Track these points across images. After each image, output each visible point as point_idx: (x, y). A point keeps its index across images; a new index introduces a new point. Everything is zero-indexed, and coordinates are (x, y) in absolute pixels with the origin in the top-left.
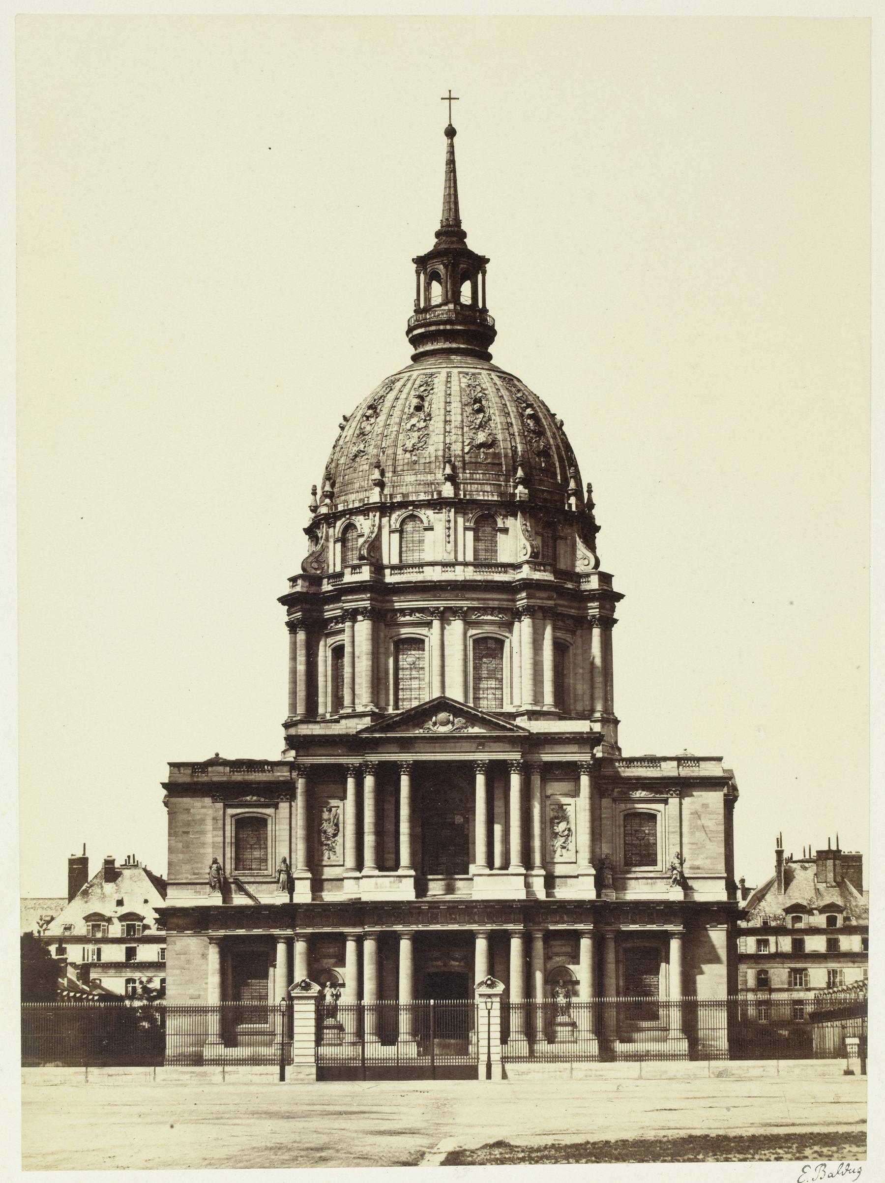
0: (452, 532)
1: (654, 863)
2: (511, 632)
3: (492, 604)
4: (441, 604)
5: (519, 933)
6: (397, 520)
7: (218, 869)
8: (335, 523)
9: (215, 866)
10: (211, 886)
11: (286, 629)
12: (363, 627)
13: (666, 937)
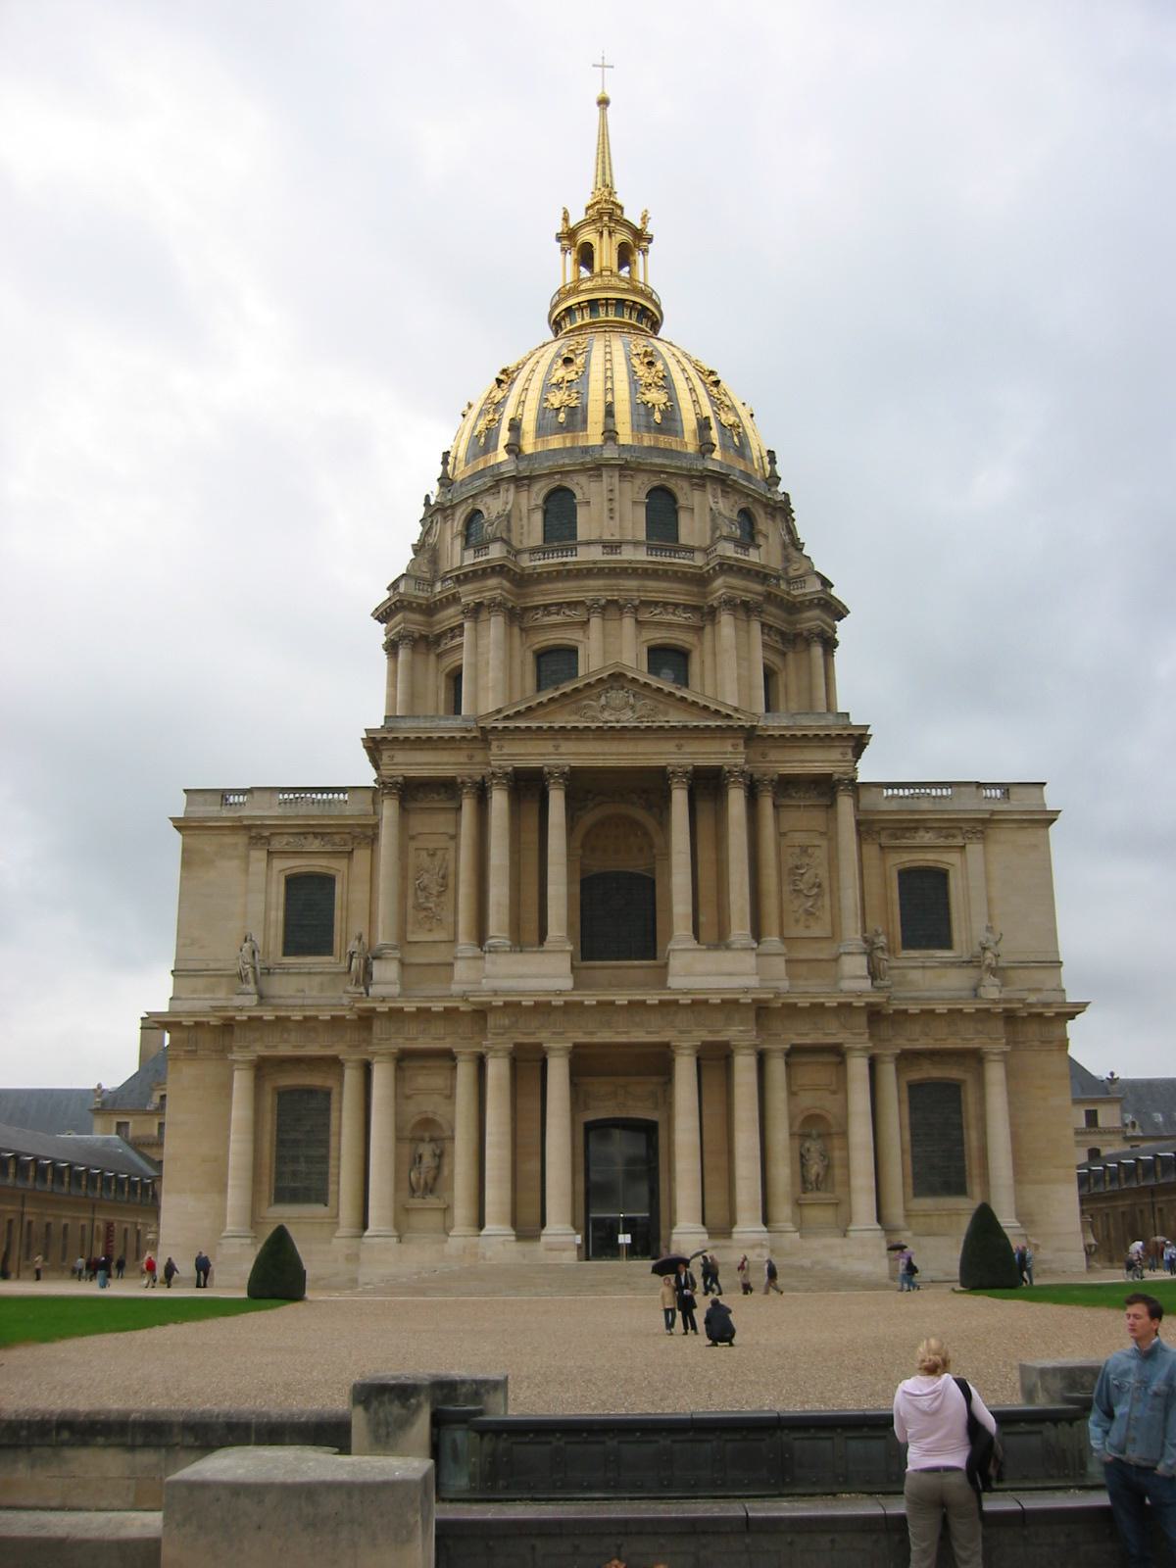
1: (946, 943)
2: (701, 641)
4: (605, 596)
5: (747, 1048)
6: (537, 494)
7: (254, 953)
8: (453, 514)
9: (247, 945)
11: (383, 656)
13: (975, 1058)
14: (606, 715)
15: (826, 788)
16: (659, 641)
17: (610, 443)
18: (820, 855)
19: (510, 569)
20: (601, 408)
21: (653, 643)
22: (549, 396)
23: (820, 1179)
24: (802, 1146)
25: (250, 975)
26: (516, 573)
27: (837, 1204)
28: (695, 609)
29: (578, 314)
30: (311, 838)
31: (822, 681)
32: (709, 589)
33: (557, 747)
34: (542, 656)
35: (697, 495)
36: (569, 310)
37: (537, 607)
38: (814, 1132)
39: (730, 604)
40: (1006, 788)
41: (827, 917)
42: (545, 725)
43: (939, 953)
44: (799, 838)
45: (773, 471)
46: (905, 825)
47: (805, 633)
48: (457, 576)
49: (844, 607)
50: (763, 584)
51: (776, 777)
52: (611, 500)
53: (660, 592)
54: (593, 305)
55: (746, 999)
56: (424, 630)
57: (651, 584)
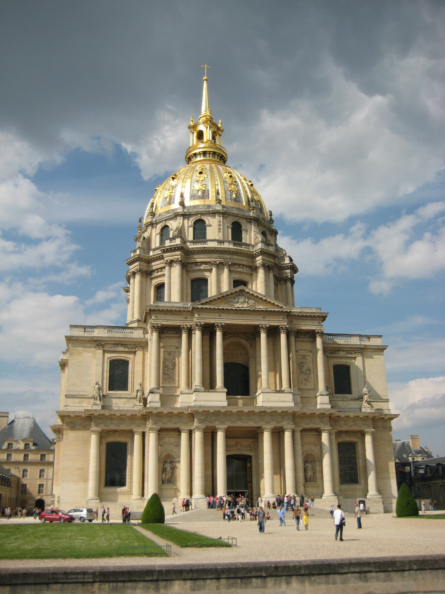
0: (221, 227)
1: (350, 392)
3: (242, 262)
4: (218, 261)
5: (290, 429)
8: (156, 227)
9: (97, 386)
10: (95, 399)
12: (176, 270)
14: (238, 304)
15: (312, 335)
16: (237, 278)
17: (218, 204)
18: (309, 359)
19: (184, 248)
20: (214, 190)
21: (235, 279)
22: (195, 185)
23: (312, 477)
24: (305, 465)
25: (98, 398)
26: (186, 250)
27: (318, 486)
28: (250, 267)
29: (198, 156)
30: (120, 345)
31: (291, 295)
32: (255, 260)
33: (220, 316)
34: (194, 281)
35: (248, 225)
36: (195, 155)
37: (193, 263)
38: (309, 460)
39: (263, 265)
40: (369, 337)
41: (313, 382)
42: (216, 308)
43: (347, 395)
44: (302, 353)
45: (271, 219)
46: (335, 349)
47: (285, 278)
48: (164, 250)
49: (297, 269)
50: (274, 259)
51: (296, 330)
52: (220, 225)
53: (239, 260)
54: (204, 153)
55: (290, 411)
56: (146, 269)
57: (235, 257)
